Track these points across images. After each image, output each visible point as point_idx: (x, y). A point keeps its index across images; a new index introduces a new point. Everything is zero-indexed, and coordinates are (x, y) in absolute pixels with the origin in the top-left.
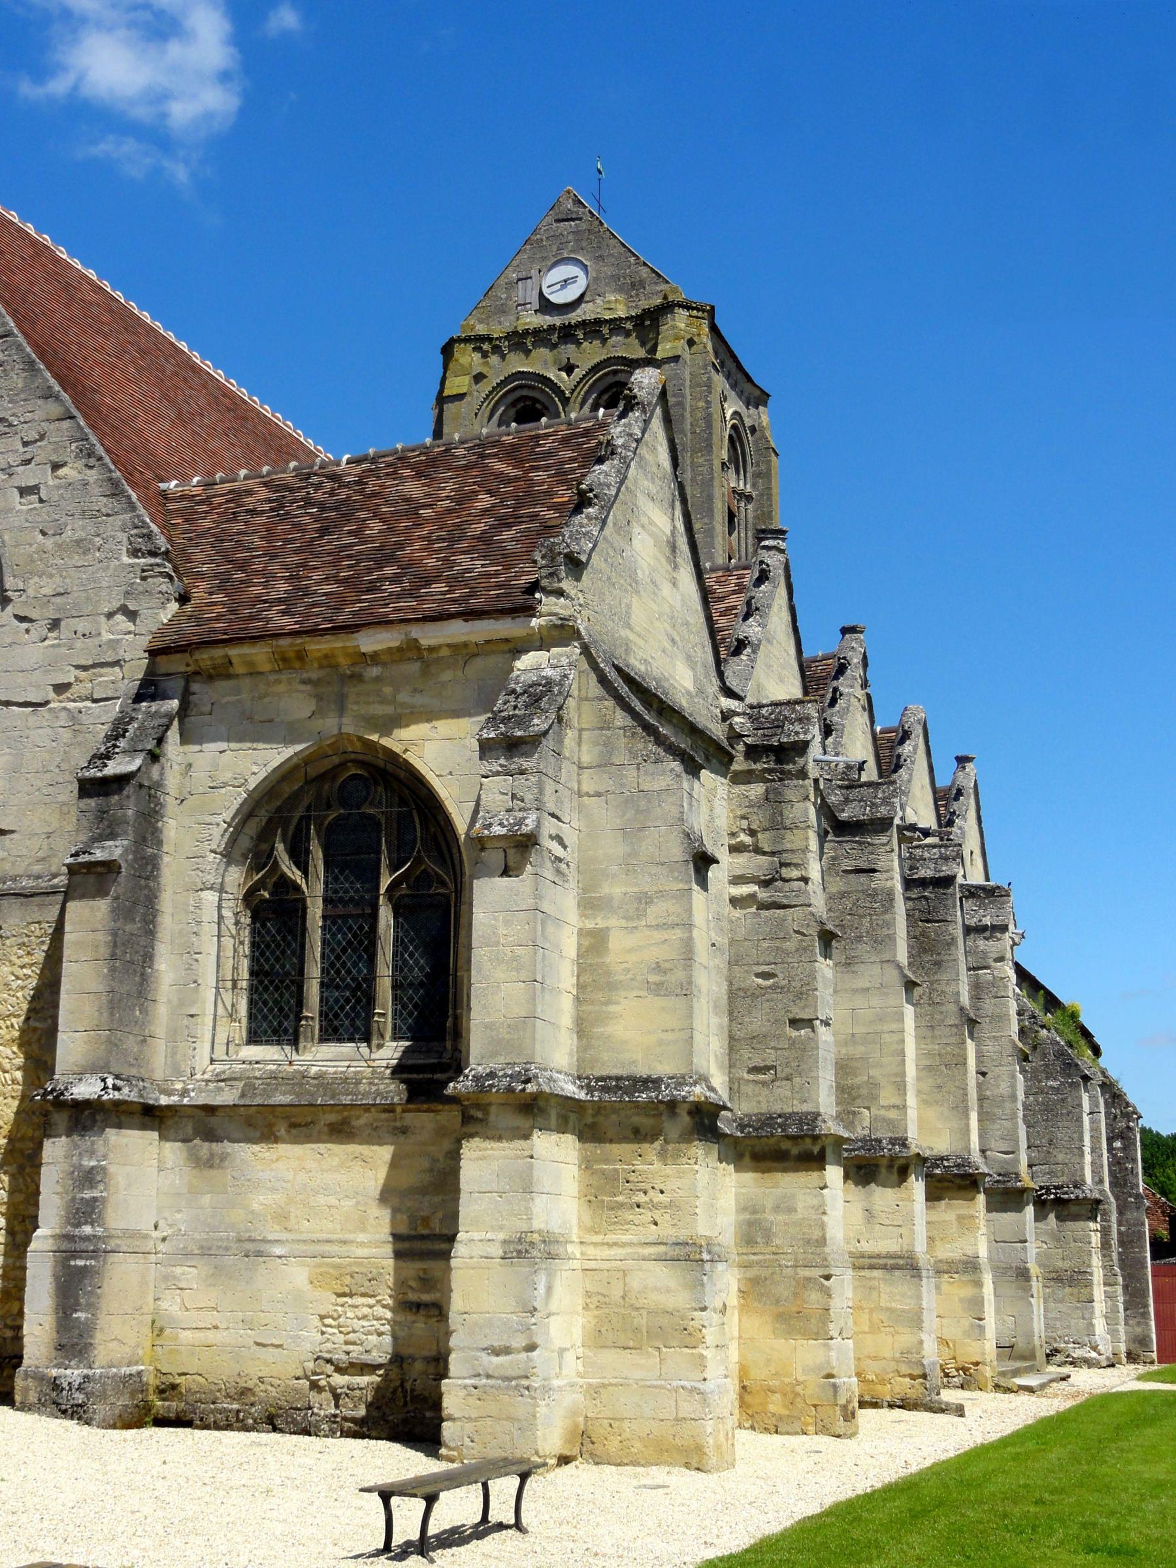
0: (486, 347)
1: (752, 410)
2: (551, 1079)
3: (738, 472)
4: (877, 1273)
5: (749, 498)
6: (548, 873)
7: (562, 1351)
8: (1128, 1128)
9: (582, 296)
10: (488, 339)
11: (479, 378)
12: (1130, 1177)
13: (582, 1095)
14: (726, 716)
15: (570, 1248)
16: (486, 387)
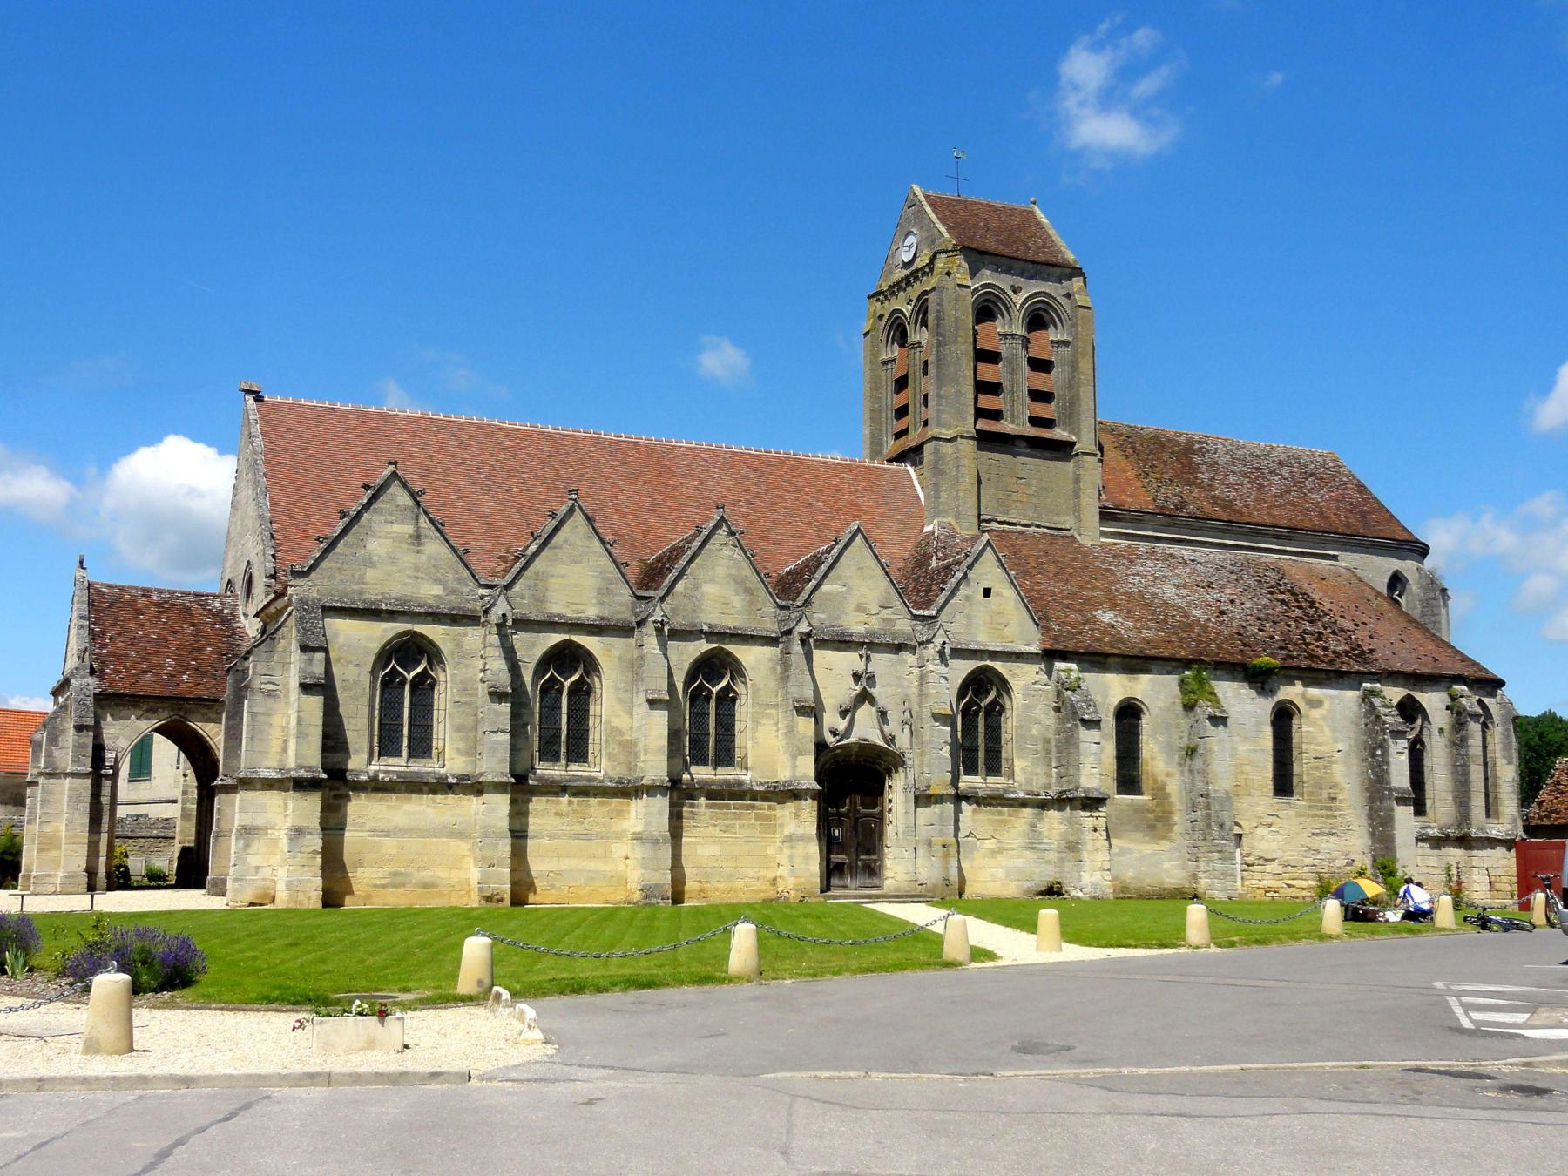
0: (881, 297)
1: (1065, 283)
2: (256, 772)
3: (1056, 328)
4: (635, 842)
5: (1066, 344)
6: (259, 697)
7: (257, 868)
8: (1385, 740)
9: (915, 254)
10: (881, 293)
11: (881, 317)
12: (1386, 776)
13: (280, 776)
14: (482, 598)
15: (269, 831)
16: (883, 322)
